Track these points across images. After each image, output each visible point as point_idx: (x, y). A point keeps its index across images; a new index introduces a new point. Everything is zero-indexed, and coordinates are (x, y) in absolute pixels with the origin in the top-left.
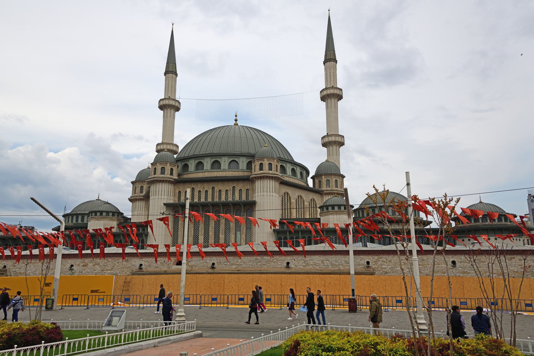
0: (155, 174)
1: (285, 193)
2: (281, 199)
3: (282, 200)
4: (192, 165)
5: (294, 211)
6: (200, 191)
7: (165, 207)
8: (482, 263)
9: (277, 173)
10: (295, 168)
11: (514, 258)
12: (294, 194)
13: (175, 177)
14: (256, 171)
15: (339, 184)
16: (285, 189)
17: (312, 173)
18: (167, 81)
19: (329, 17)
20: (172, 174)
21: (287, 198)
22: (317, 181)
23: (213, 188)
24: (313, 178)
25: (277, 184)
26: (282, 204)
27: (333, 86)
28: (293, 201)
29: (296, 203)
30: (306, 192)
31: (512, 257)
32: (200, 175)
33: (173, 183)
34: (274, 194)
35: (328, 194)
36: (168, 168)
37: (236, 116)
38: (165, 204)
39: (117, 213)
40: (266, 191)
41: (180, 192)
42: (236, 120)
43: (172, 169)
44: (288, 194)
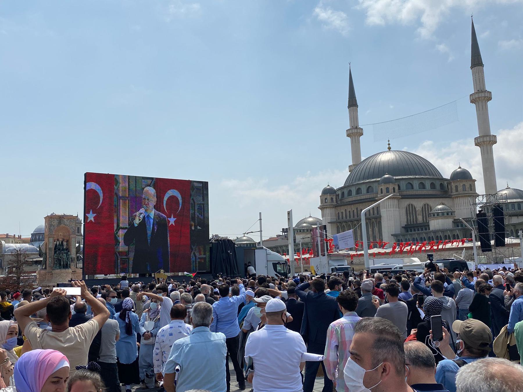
1: (409, 205)
6: (350, 211)
8: (442, 256)
11: (458, 252)
13: (335, 203)
16: (406, 202)
19: (473, 23)
23: (357, 208)
27: (478, 91)
31: (457, 251)
32: (350, 199)
33: (333, 208)
37: (389, 141)
40: (386, 208)
41: (338, 213)
42: (389, 144)
44: (412, 205)
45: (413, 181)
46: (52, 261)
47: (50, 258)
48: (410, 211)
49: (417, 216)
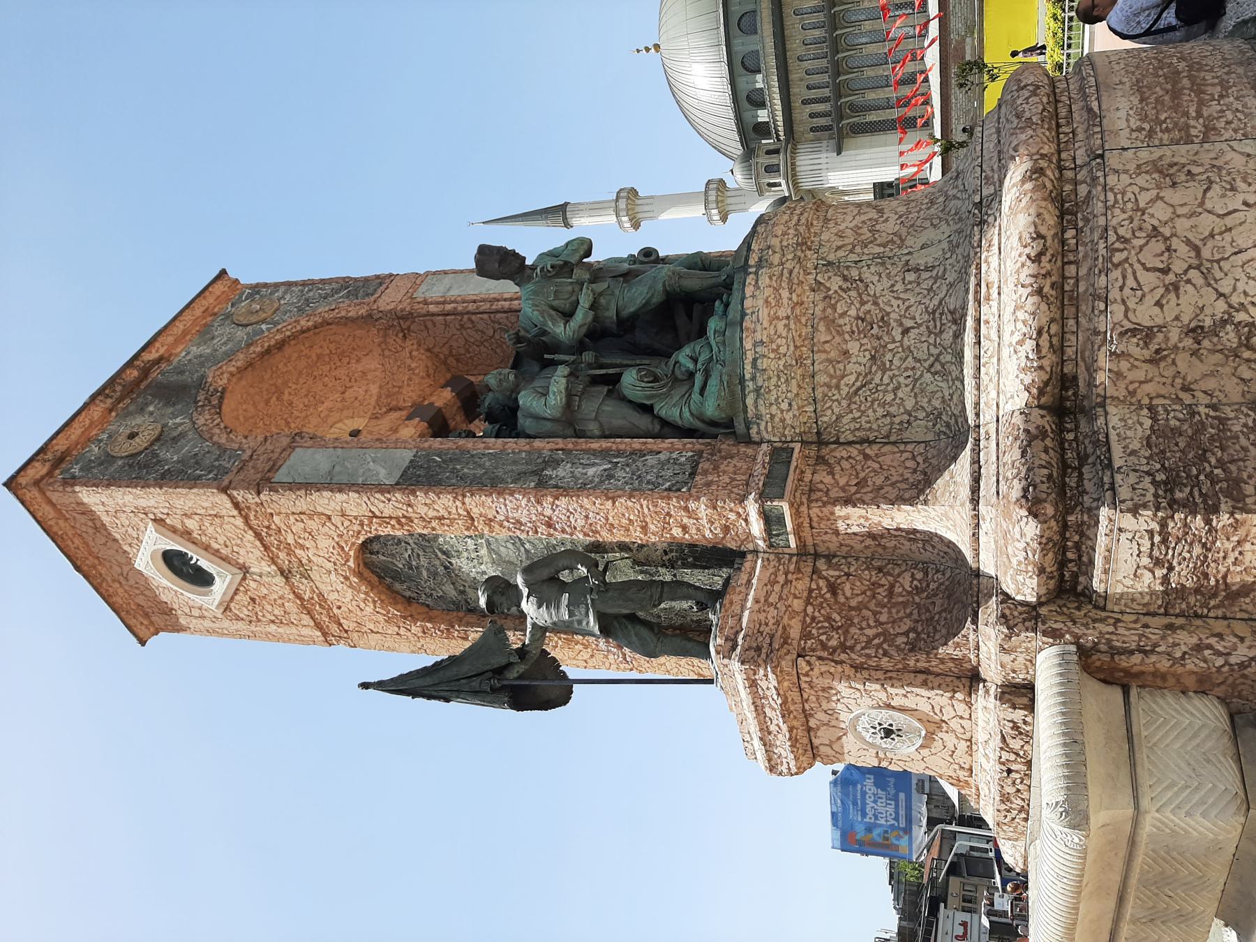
7: (843, 153)
46: (604, 454)
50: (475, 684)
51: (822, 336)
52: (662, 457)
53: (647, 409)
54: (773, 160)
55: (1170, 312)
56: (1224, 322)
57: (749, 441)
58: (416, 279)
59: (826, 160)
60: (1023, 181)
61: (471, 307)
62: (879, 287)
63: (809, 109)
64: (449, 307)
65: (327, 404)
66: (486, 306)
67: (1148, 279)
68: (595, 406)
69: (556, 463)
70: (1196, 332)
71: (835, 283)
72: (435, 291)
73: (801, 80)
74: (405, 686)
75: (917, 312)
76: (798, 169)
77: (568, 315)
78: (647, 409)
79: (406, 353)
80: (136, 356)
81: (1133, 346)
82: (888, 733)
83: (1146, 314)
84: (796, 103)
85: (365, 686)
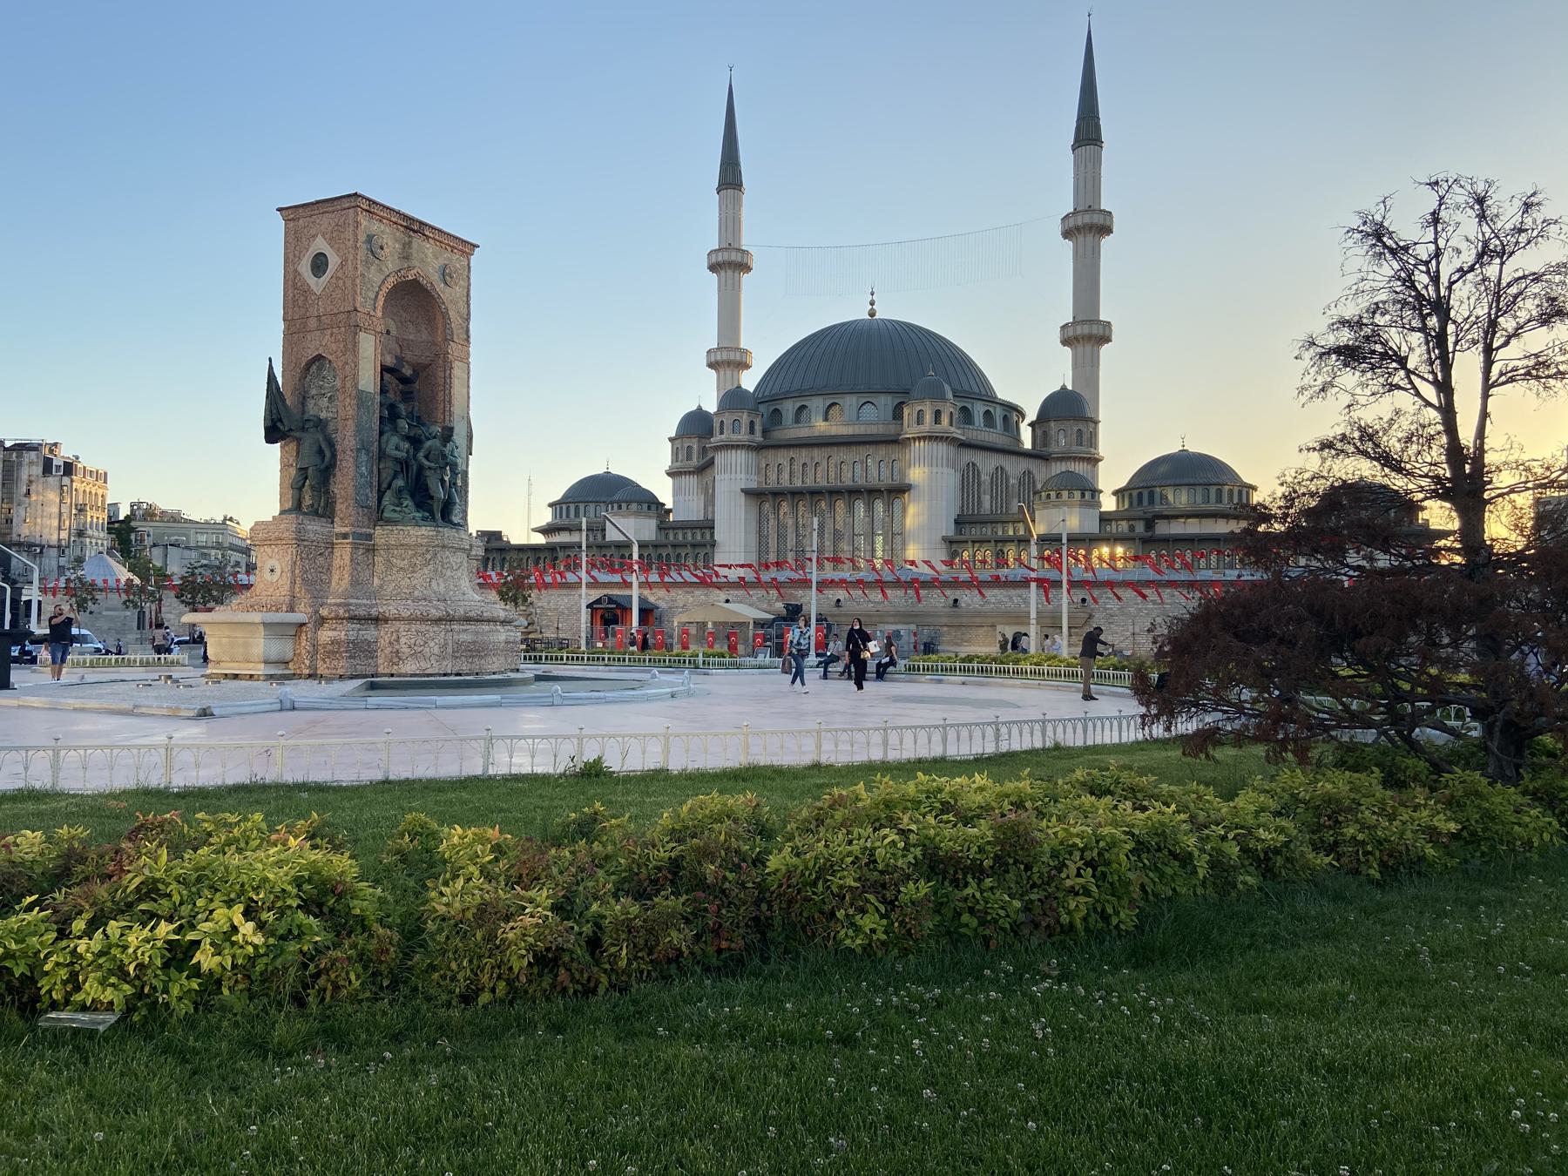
0: (722, 433)
2: (959, 475)
3: (963, 479)
4: (789, 408)
5: (986, 499)
9: (952, 429)
10: (992, 410)
12: (987, 464)
13: (758, 437)
14: (910, 430)
15: (1085, 437)
16: (968, 456)
17: (1032, 415)
18: (724, 207)
20: (752, 431)
21: (974, 473)
22: (1039, 432)
24: (1032, 425)
25: (952, 449)
26: (963, 487)
28: (985, 478)
29: (992, 483)
30: (1014, 458)
32: (802, 432)
34: (945, 470)
35: (1061, 459)
36: (745, 419)
38: (742, 490)
39: (648, 502)
42: (872, 303)
43: (752, 423)
45: (973, 404)
46: (371, 472)
47: (364, 457)
48: (969, 480)
49: (982, 496)
50: (274, 411)
51: (410, 552)
52: (370, 495)
53: (389, 487)
54: (745, 428)
55: (404, 646)
56: (400, 659)
57: (375, 526)
58: (465, 359)
59: (738, 478)
60: (447, 612)
61: (447, 392)
62: (426, 570)
63: (786, 463)
64: (448, 381)
65: (404, 314)
66: (447, 399)
67: (413, 641)
68: (389, 467)
69: (367, 454)
70: (397, 652)
71: (429, 557)
72: (457, 371)
73: (812, 458)
74: (271, 378)
75: (416, 582)
76: (734, 451)
77: (427, 457)
78: (389, 487)
79: (428, 354)
80: (426, 225)
81: (394, 637)
82: (272, 571)
83: (403, 640)
84: (792, 453)
85: (270, 360)
